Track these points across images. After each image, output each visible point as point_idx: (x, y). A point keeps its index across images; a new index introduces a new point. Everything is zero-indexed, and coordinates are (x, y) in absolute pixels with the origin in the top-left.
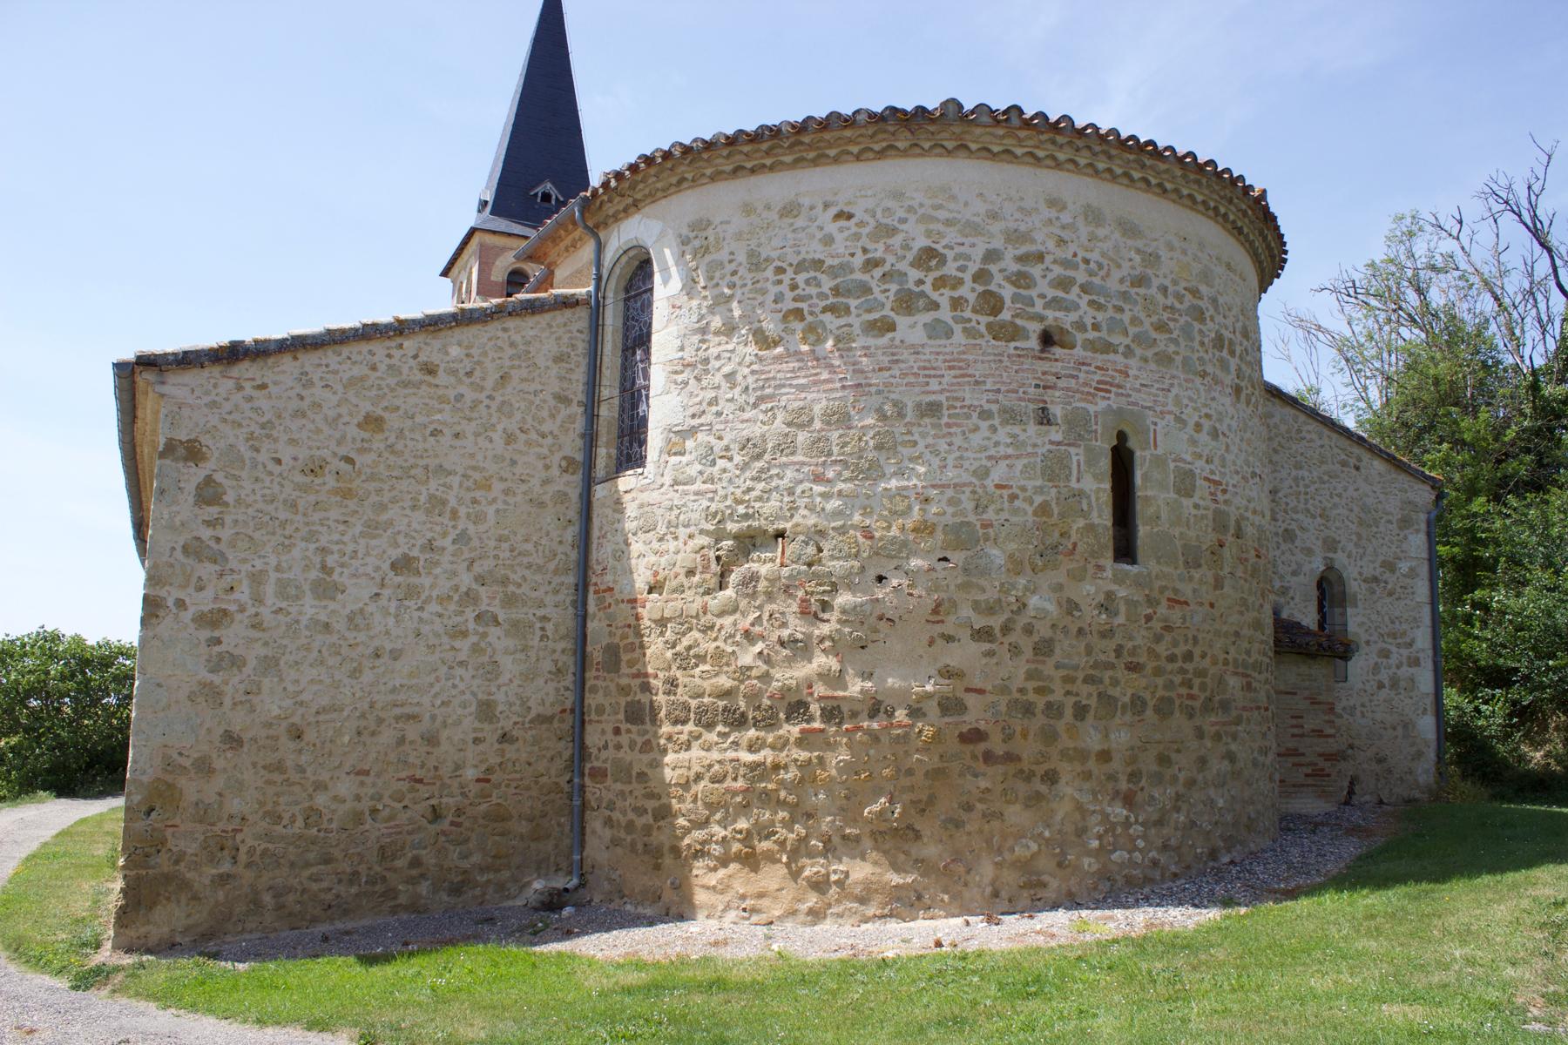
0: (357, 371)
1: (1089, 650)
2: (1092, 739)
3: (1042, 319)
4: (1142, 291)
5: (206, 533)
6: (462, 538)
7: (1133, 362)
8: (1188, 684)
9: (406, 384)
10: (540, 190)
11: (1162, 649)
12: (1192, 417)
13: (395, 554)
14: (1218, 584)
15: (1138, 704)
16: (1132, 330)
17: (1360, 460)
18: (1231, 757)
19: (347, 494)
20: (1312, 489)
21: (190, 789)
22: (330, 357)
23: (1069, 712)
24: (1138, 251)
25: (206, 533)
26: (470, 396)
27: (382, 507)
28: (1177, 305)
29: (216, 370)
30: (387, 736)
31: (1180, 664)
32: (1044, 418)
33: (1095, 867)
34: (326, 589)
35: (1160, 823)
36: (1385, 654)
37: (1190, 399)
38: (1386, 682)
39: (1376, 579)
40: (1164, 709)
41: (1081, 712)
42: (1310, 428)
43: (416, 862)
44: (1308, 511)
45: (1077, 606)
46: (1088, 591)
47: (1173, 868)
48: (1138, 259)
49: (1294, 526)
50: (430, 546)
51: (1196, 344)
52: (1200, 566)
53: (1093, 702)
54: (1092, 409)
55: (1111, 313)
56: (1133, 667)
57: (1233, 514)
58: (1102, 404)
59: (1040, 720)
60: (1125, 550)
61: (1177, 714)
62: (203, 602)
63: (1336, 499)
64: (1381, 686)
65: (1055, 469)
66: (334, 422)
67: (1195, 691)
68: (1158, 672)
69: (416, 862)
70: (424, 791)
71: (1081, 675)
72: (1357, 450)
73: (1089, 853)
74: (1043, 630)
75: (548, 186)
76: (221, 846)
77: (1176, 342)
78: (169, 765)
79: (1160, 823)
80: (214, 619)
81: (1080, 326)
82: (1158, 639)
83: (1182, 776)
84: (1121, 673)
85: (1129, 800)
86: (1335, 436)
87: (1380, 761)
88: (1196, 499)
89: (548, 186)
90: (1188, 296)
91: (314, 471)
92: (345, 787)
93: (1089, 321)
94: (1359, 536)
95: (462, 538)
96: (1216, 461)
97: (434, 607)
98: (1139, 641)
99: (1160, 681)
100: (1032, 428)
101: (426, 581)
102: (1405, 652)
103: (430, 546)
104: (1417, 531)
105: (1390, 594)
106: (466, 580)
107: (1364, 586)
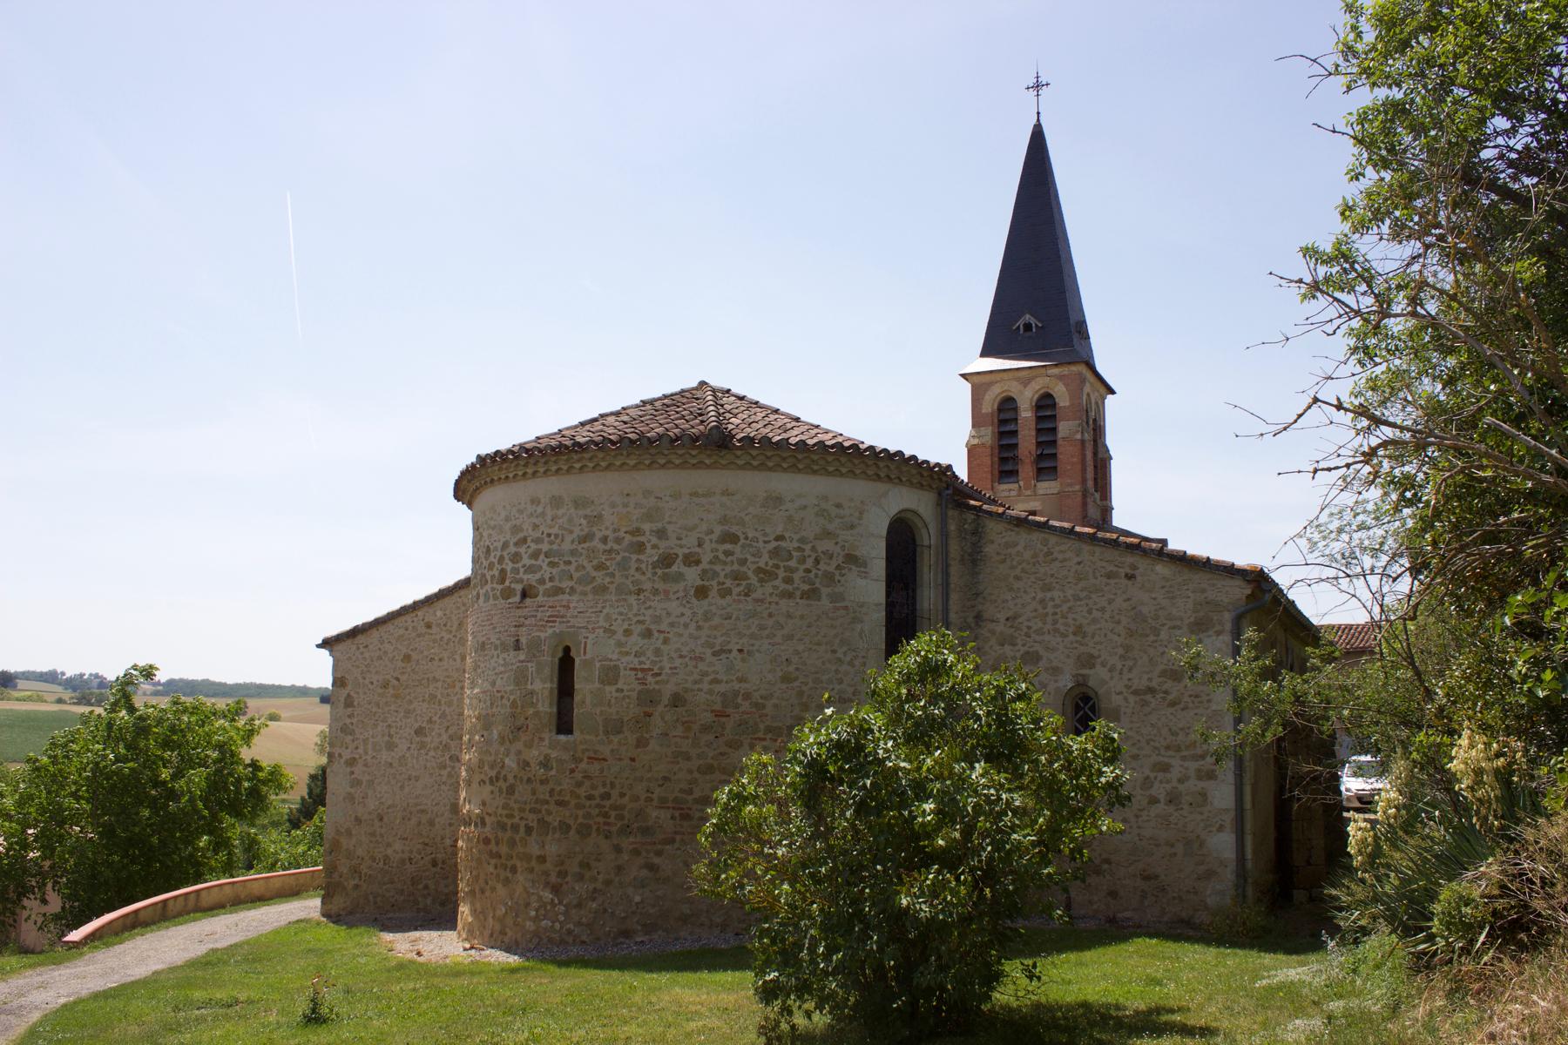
0: (401, 631)
1: (534, 793)
2: (535, 850)
3: (521, 581)
4: (586, 545)
5: (348, 721)
6: (443, 715)
7: (575, 598)
8: (606, 815)
9: (419, 636)
10: (1021, 323)
11: (582, 792)
12: (619, 627)
13: (416, 726)
14: (641, 743)
15: (565, 827)
16: (576, 575)
17: (1134, 567)
18: (652, 867)
19: (396, 696)
20: (1065, 608)
21: (344, 841)
22: (390, 627)
23: (522, 829)
24: (586, 517)
25: (348, 721)
26: (447, 637)
27: (411, 702)
28: (616, 547)
29: (349, 642)
30: (414, 821)
31: (598, 801)
32: (517, 646)
33: (533, 928)
34: (391, 746)
35: (579, 906)
36: (1165, 768)
37: (621, 614)
38: (1162, 797)
39: (1151, 690)
40: (584, 831)
41: (529, 830)
42: (1063, 548)
43: (426, 887)
44: (1056, 630)
45: (528, 764)
46: (534, 755)
47: (584, 938)
48: (584, 522)
49: (1037, 647)
50: (430, 721)
51: (632, 571)
52: (619, 732)
53: (534, 824)
54: (543, 635)
55: (562, 567)
56: (560, 803)
57: (668, 690)
58: (550, 631)
59: (509, 834)
60: (564, 724)
61: (594, 834)
62: (347, 755)
63: (1096, 614)
64: (1154, 801)
65: (520, 678)
66: (392, 660)
67: (612, 820)
68: (579, 806)
69: (426, 887)
70: (429, 850)
71: (528, 807)
72: (1129, 559)
73: (530, 919)
74: (511, 780)
75: (1028, 317)
76: (355, 871)
77: (612, 575)
78: (338, 831)
79: (579, 906)
80: (352, 762)
81: (542, 581)
82: (579, 784)
83: (601, 877)
84: (552, 807)
85: (556, 889)
86: (1098, 550)
87: (1147, 878)
88: (620, 686)
89: (1028, 317)
90: (628, 538)
91: (385, 686)
92: (398, 846)
93: (547, 576)
94: (1128, 648)
95: (443, 715)
96: (649, 654)
97: (432, 753)
98: (565, 786)
99: (580, 813)
100: (512, 653)
101: (428, 739)
102: (1193, 766)
103: (430, 721)
104: (1219, 633)
105: (1173, 704)
106: (445, 737)
107: (1132, 699)
